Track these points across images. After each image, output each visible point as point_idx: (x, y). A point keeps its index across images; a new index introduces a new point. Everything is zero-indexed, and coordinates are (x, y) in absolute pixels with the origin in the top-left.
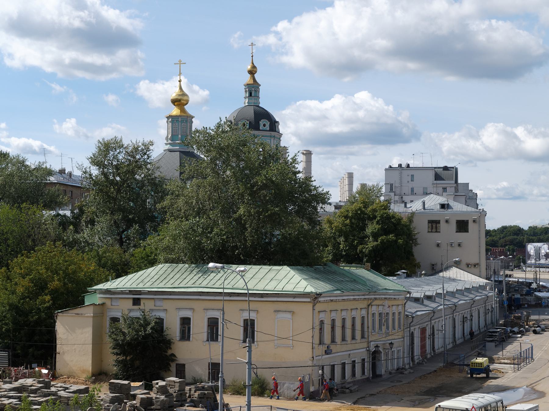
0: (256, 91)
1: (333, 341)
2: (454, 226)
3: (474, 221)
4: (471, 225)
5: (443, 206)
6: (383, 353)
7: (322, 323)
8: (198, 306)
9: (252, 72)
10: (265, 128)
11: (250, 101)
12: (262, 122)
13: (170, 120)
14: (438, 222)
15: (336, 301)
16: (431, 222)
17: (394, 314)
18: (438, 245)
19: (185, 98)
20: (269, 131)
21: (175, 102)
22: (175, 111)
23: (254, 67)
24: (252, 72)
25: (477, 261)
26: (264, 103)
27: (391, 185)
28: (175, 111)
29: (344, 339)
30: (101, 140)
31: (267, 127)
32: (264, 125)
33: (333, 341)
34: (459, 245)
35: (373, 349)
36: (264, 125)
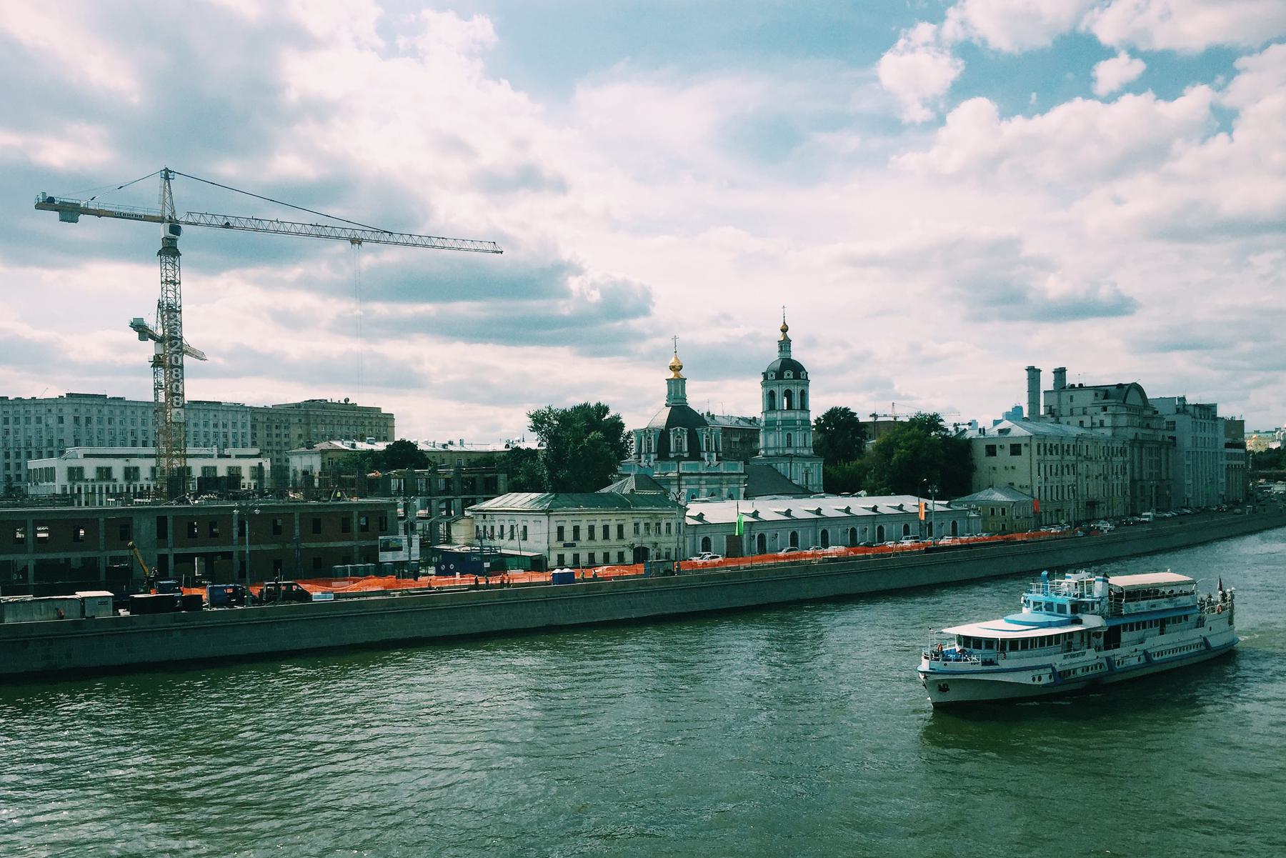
4: (1024, 450)
6: (651, 550)
8: (506, 518)
10: (788, 377)
12: (786, 373)
17: (668, 524)
20: (794, 379)
21: (673, 368)
22: (672, 375)
24: (785, 330)
26: (795, 356)
27: (1050, 407)
28: (672, 375)
32: (788, 375)
36: (788, 375)
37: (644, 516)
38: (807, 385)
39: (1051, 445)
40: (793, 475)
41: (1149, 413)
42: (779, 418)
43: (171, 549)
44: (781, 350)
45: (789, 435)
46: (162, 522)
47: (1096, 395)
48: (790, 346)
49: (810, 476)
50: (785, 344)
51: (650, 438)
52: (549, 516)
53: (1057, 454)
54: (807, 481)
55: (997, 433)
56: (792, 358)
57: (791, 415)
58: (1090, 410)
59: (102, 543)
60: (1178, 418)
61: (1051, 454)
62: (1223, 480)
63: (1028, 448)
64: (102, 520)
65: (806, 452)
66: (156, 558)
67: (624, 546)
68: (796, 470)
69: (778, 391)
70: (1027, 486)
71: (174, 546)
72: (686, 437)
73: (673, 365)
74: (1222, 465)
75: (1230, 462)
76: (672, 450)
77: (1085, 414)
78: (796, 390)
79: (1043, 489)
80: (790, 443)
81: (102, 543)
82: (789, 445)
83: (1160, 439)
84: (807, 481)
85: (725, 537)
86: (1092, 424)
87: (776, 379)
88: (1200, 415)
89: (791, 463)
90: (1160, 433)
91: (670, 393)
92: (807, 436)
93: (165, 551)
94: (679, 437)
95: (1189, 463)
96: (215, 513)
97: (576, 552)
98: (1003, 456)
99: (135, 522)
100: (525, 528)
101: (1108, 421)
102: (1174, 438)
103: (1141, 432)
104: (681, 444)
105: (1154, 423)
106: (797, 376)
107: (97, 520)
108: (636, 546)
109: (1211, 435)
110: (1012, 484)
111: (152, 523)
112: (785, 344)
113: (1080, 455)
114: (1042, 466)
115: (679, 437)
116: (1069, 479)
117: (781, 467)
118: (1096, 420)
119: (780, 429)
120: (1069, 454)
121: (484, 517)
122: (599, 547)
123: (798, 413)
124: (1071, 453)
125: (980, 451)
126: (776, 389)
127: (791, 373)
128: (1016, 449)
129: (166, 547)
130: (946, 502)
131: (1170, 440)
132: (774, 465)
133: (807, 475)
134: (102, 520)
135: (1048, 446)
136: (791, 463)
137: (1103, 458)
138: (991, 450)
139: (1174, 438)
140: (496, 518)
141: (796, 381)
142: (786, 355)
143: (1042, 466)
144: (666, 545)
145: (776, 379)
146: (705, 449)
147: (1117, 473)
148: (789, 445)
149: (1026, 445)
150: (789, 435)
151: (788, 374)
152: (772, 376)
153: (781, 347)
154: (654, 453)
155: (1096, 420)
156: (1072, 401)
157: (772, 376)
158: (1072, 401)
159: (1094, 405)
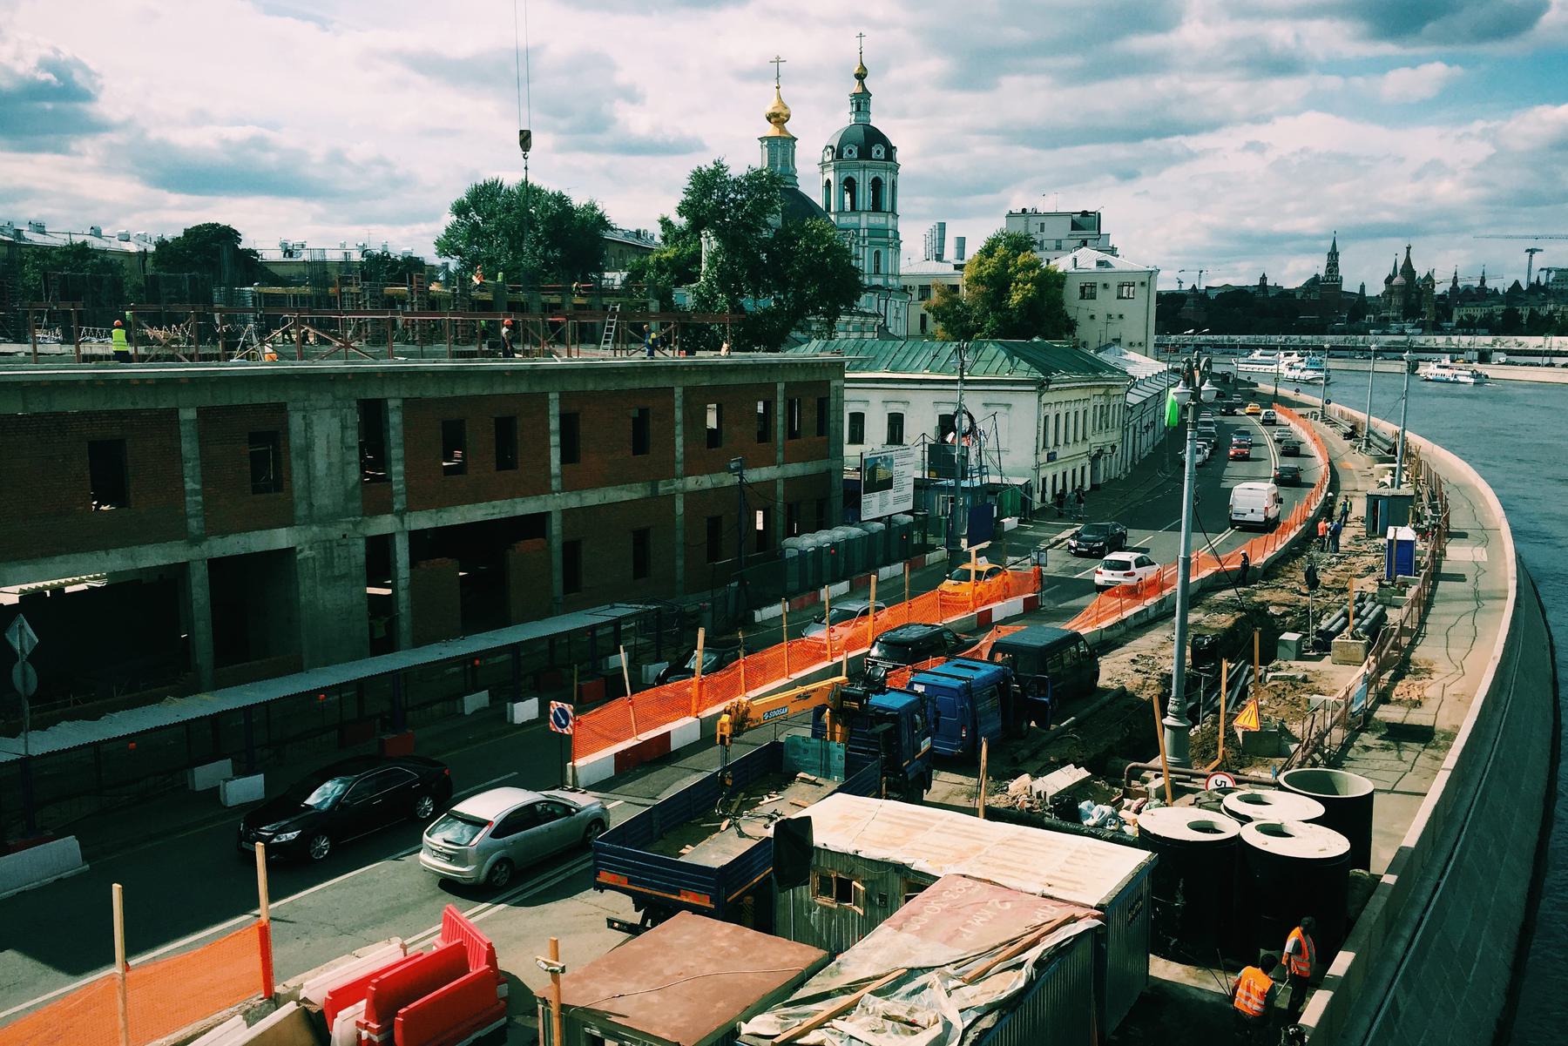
0: (865, 103)
1: (1056, 444)
5: (1100, 263)
7: (1046, 417)
11: (858, 118)
12: (874, 150)
13: (766, 143)
14: (1093, 286)
15: (1062, 389)
18: (1092, 317)
25: (1141, 338)
26: (875, 122)
29: (1075, 440)
32: (878, 152)
33: (1056, 444)
35: (1094, 452)
36: (878, 152)
42: (863, 225)
43: (401, 514)
45: (877, 254)
46: (372, 416)
50: (861, 101)
55: (1093, 266)
59: (193, 503)
63: (1145, 289)
64: (188, 414)
66: (360, 549)
69: (863, 180)
70: (1140, 344)
71: (410, 508)
73: (777, 111)
80: (878, 267)
81: (193, 503)
82: (877, 272)
87: (860, 158)
89: (887, 301)
93: (385, 524)
96: (509, 389)
99: (296, 422)
107: (174, 412)
110: (1131, 344)
111: (344, 428)
112: (861, 101)
119: (867, 242)
125: (1071, 293)
126: (855, 175)
127: (882, 152)
129: (387, 508)
134: (188, 414)
136: (887, 301)
138: (1088, 292)
145: (860, 158)
149: (1143, 284)
150: (877, 254)
151: (878, 150)
152: (850, 152)
157: (850, 152)
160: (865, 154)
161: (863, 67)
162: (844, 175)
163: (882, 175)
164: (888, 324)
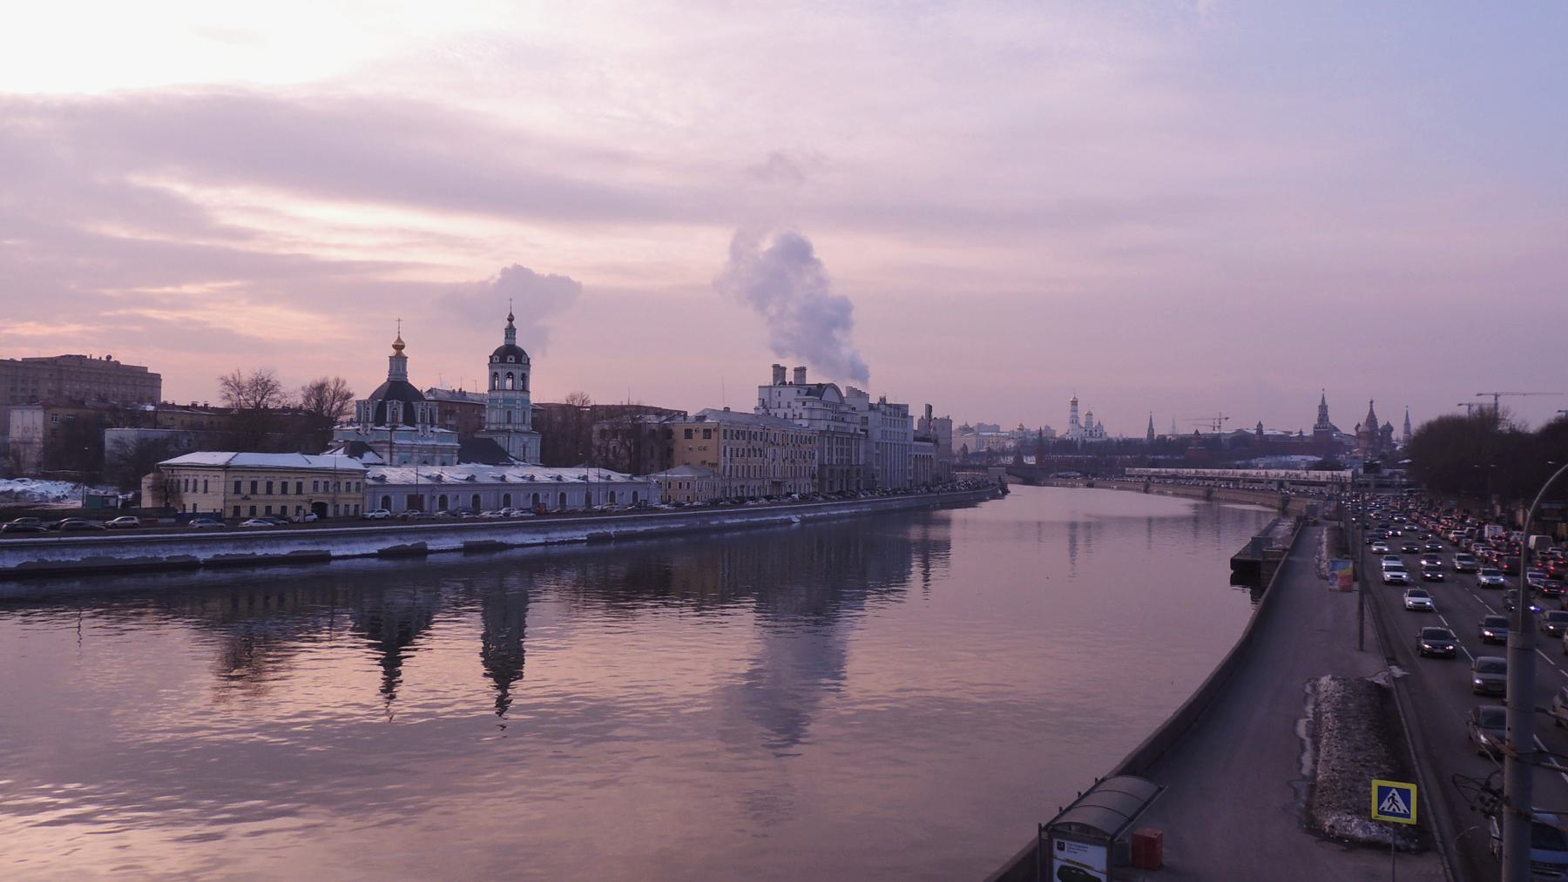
2: (702, 434)
3: (714, 430)
8: (191, 473)
9: (511, 319)
14: (691, 430)
16: (687, 430)
17: (348, 483)
18: (690, 449)
19: (401, 344)
23: (511, 315)
24: (511, 319)
26: (518, 343)
27: (764, 400)
30: (230, 379)
31: (513, 361)
34: (704, 449)
37: (323, 475)
38: (529, 369)
39: (738, 432)
40: (511, 446)
41: (844, 409)
44: (506, 338)
47: (799, 392)
48: (514, 334)
49: (527, 450)
50: (510, 331)
51: (368, 409)
52: (226, 472)
53: (744, 439)
54: (524, 454)
56: (517, 344)
57: (512, 395)
58: (794, 404)
60: (871, 415)
61: (738, 438)
62: (912, 467)
65: (524, 428)
67: (302, 501)
68: (514, 444)
72: (401, 410)
74: (911, 455)
75: (918, 453)
76: (388, 420)
77: (789, 407)
78: (517, 373)
79: (728, 468)
82: (509, 422)
83: (852, 431)
84: (524, 454)
85: (406, 496)
86: (794, 415)
87: (500, 362)
88: (891, 413)
90: (853, 426)
91: (391, 369)
92: (527, 414)
94: (395, 409)
95: (878, 452)
97: (253, 504)
98: (698, 439)
100: (206, 481)
101: (806, 414)
102: (866, 431)
103: (833, 425)
104: (397, 415)
105: (848, 419)
106: (518, 361)
108: (313, 502)
109: (901, 430)
112: (510, 331)
113: (766, 441)
114: (728, 449)
115: (395, 409)
116: (755, 461)
117: (500, 440)
118: (797, 413)
120: (756, 440)
121: (173, 471)
122: (261, 501)
123: (518, 393)
124: (758, 439)
125: (679, 433)
126: (499, 371)
128: (707, 433)
130: (629, 475)
131: (863, 433)
132: (495, 439)
133: (524, 448)
135: (735, 432)
137: (791, 445)
138: (688, 434)
139: (866, 431)
140: (182, 473)
141: (517, 365)
142: (510, 342)
143: (728, 449)
144: (347, 502)
145: (500, 362)
146: (419, 421)
147: (804, 458)
148: (509, 422)
153: (507, 334)
154: (372, 422)
155: (797, 413)
156: (779, 395)
158: (779, 395)
159: (796, 400)
160: (503, 360)
161: (511, 315)
162: (494, 371)
163: (513, 371)
164: (510, 450)
